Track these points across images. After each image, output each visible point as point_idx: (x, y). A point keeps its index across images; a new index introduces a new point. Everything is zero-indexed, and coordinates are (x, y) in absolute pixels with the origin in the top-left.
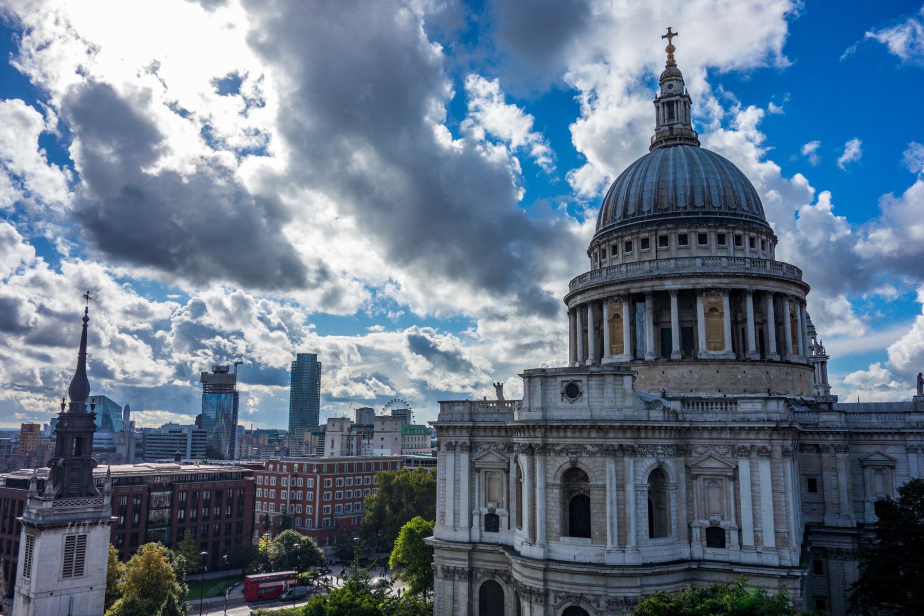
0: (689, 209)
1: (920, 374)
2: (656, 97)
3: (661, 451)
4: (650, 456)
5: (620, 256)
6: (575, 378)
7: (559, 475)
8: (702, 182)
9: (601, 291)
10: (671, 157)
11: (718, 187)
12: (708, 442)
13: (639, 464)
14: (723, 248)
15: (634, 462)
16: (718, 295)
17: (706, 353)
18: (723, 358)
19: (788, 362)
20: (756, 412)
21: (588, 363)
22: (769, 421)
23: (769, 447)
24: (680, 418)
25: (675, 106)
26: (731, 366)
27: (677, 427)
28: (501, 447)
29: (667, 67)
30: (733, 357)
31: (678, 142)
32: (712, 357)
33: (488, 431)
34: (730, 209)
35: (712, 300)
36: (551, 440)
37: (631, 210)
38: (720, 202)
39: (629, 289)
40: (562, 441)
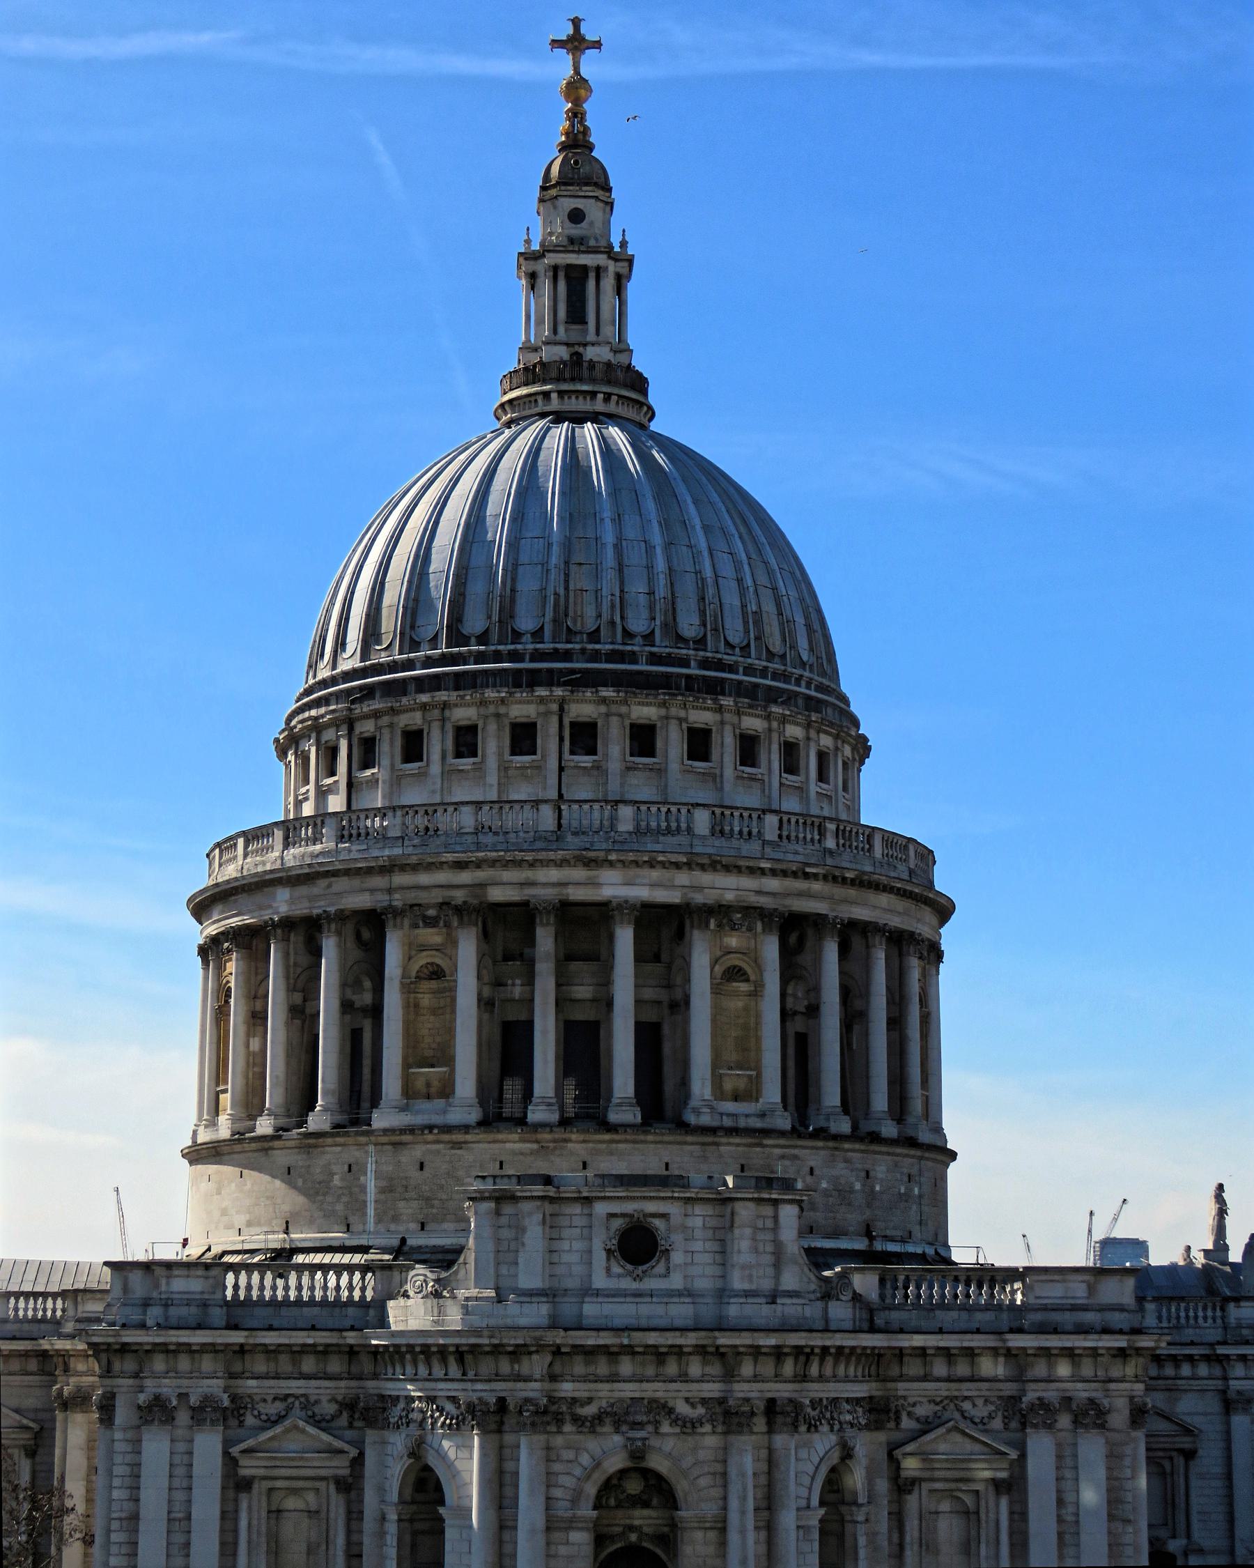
0: (662, 647)
1: (1220, 1187)
2: (528, 242)
3: (848, 1417)
4: (825, 1428)
5: (435, 768)
6: (651, 1207)
7: (591, 1490)
8: (696, 557)
9: (379, 881)
10: (595, 461)
11: (740, 581)
12: (943, 1389)
13: (803, 1454)
14: (752, 778)
15: (796, 1448)
16: (750, 929)
17: (712, 1108)
18: (757, 1123)
19: (912, 1142)
20: (1074, 1308)
21: (317, 1120)
22: (1106, 1331)
23: (1106, 1402)
24: (879, 1321)
25: (591, 284)
26: (777, 1151)
27: (874, 1348)
28: (329, 1409)
29: (564, 147)
30: (784, 1121)
31: (599, 405)
32: (727, 1122)
33: (284, 1358)
34: (771, 656)
35: (733, 941)
36: (567, 1388)
37: (475, 623)
38: (747, 631)
39: (482, 886)
40: (604, 1390)
